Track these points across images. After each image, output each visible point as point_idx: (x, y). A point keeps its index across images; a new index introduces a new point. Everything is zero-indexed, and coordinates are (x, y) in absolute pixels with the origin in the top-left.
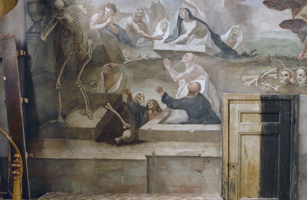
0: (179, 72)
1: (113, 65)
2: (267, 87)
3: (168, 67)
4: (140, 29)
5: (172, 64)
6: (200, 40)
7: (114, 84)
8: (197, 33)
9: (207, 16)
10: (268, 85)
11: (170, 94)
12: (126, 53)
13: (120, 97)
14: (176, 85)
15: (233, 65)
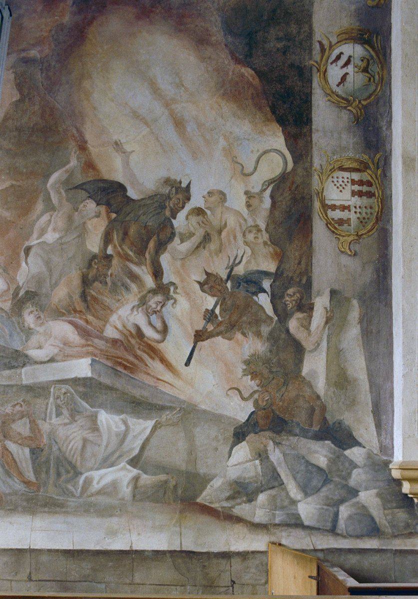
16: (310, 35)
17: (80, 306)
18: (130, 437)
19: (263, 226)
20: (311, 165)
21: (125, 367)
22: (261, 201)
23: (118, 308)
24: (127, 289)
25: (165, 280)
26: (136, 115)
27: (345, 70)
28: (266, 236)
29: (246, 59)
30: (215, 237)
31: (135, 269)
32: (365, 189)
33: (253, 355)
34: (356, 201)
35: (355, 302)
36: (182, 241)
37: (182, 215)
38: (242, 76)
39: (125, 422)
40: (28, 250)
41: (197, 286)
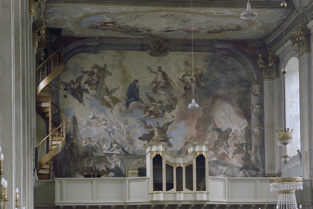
0: (112, 160)
1: (90, 158)
2: (140, 165)
3: (108, 159)
4: (99, 146)
5: (109, 158)
6: (118, 150)
7: (90, 164)
8: (117, 148)
9: (121, 142)
10: (140, 164)
11: (109, 167)
12: (94, 154)
13: (92, 168)
14: (110, 164)
15: (129, 158)
16: (251, 104)
17: (214, 149)
18: (223, 170)
19: (244, 136)
20: (251, 125)
21: (222, 159)
22: (243, 132)
23: (221, 149)
24: (222, 146)
25: (228, 145)
26: (223, 117)
27: (256, 110)
28: (244, 137)
29: (240, 109)
30: (236, 137)
31: (223, 143)
32: (260, 129)
33: (243, 157)
34: (259, 131)
35: (259, 148)
36: (231, 138)
37: (231, 134)
38: (240, 111)
39: (222, 168)
40: (206, 140)
41: (233, 146)
